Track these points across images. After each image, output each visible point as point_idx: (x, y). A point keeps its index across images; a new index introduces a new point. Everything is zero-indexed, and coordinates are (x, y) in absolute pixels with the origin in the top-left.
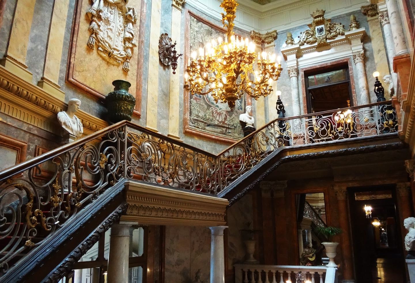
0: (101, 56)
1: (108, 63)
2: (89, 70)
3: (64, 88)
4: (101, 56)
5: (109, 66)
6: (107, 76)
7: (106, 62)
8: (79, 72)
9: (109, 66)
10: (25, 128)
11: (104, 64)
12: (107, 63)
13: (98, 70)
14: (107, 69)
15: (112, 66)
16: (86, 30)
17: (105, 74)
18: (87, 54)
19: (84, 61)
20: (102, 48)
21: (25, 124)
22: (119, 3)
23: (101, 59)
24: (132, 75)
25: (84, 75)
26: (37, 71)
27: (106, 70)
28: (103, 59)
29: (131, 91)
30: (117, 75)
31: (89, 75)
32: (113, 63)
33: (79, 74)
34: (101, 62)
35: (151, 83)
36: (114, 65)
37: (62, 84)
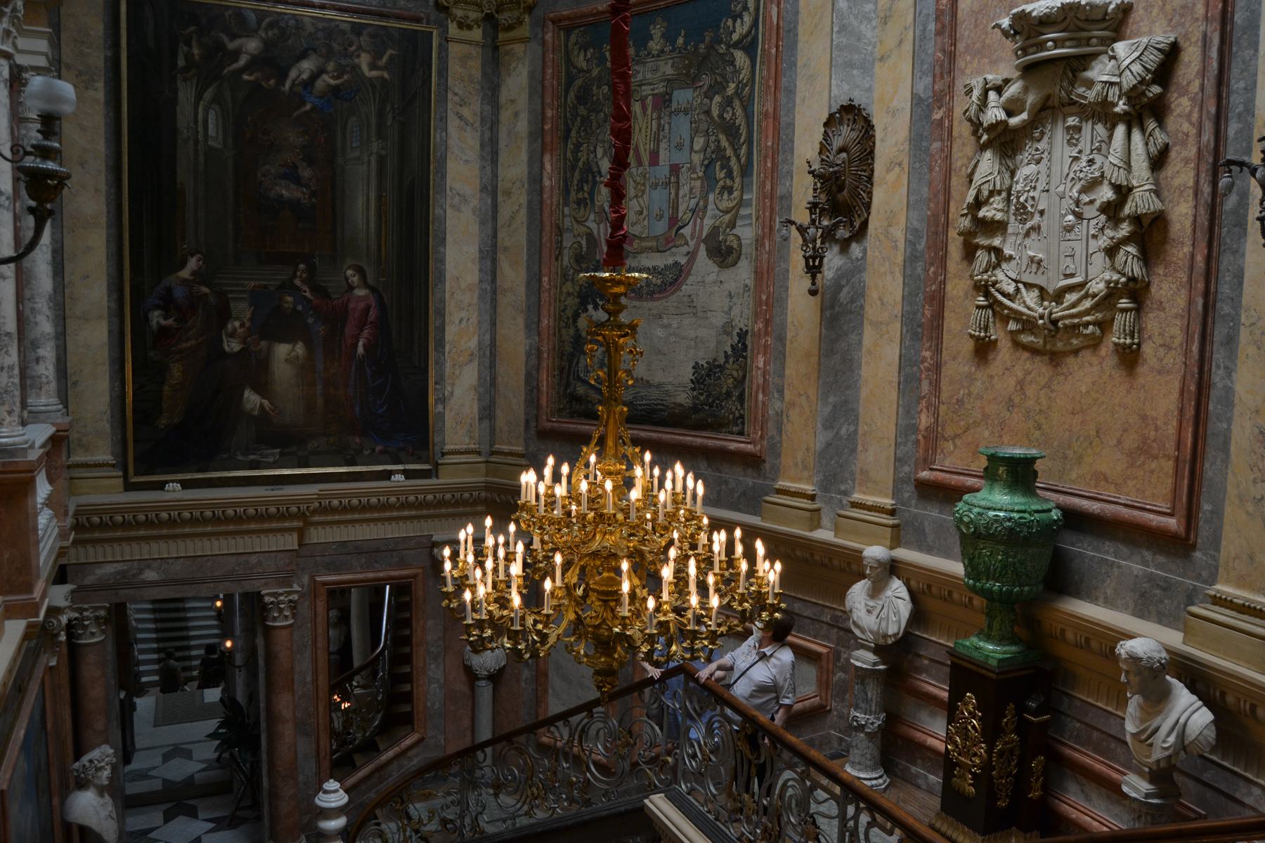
0: (1025, 347)
1: (1055, 358)
2: (985, 417)
3: (914, 502)
4: (1025, 347)
5: (1056, 366)
6: (1049, 408)
7: (1046, 358)
8: (957, 436)
9: (1056, 366)
10: (827, 618)
11: (1039, 369)
12: (1051, 360)
13: (1017, 400)
14: (1050, 379)
15: (1071, 360)
16: (966, 294)
17: (1044, 402)
18: (978, 366)
19: (969, 394)
20: (1017, 320)
21: (826, 610)
22: (1048, 97)
23: (1026, 355)
24: (1162, 351)
25: (970, 440)
26: (843, 488)
27: (1048, 386)
28: (1033, 351)
29: (1157, 429)
30: (1094, 383)
31: (987, 433)
32: (1068, 348)
33: (955, 446)
34: (1028, 365)
35: (1252, 350)
36: (1076, 352)
37: (906, 495)
